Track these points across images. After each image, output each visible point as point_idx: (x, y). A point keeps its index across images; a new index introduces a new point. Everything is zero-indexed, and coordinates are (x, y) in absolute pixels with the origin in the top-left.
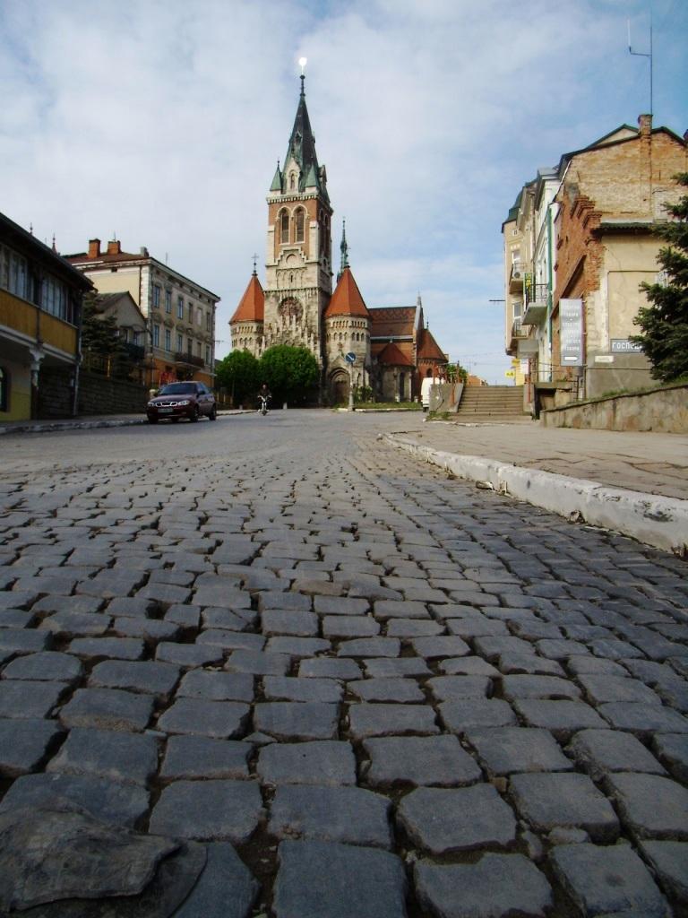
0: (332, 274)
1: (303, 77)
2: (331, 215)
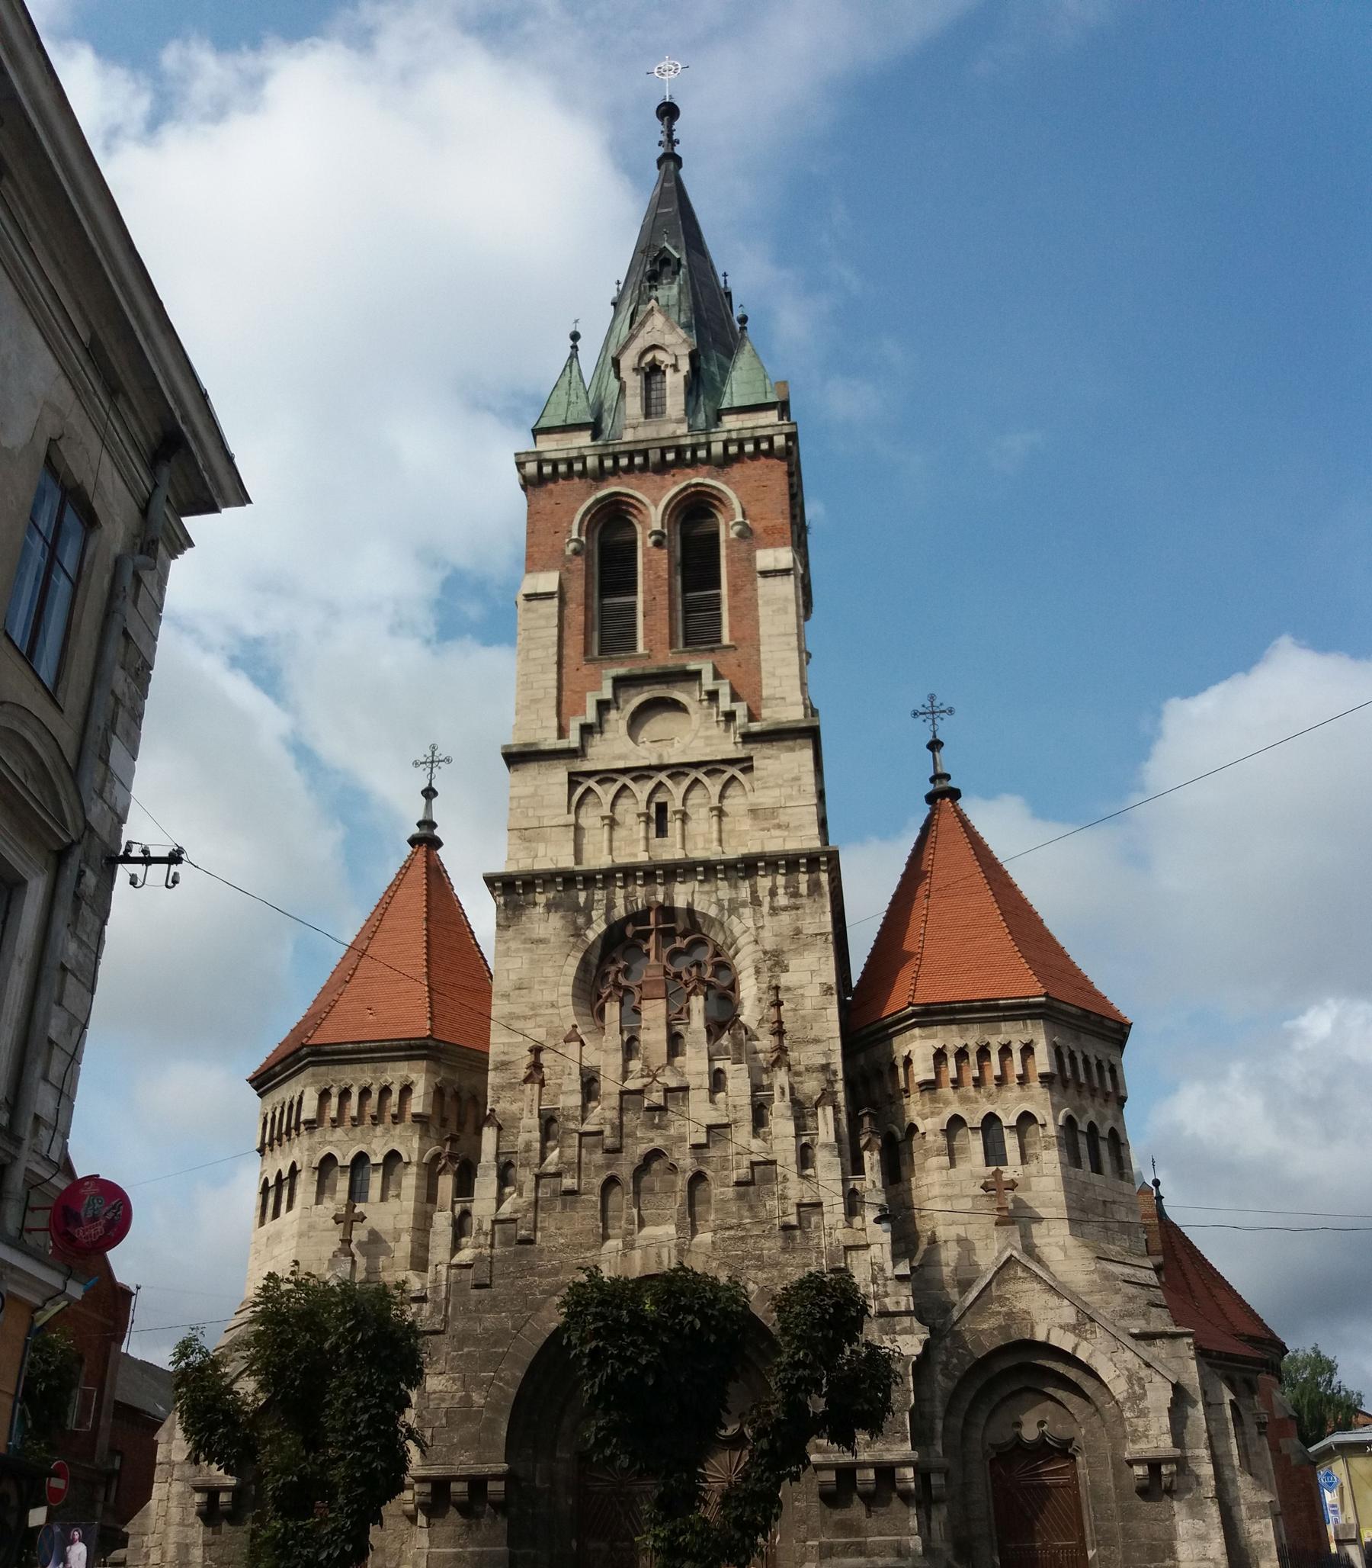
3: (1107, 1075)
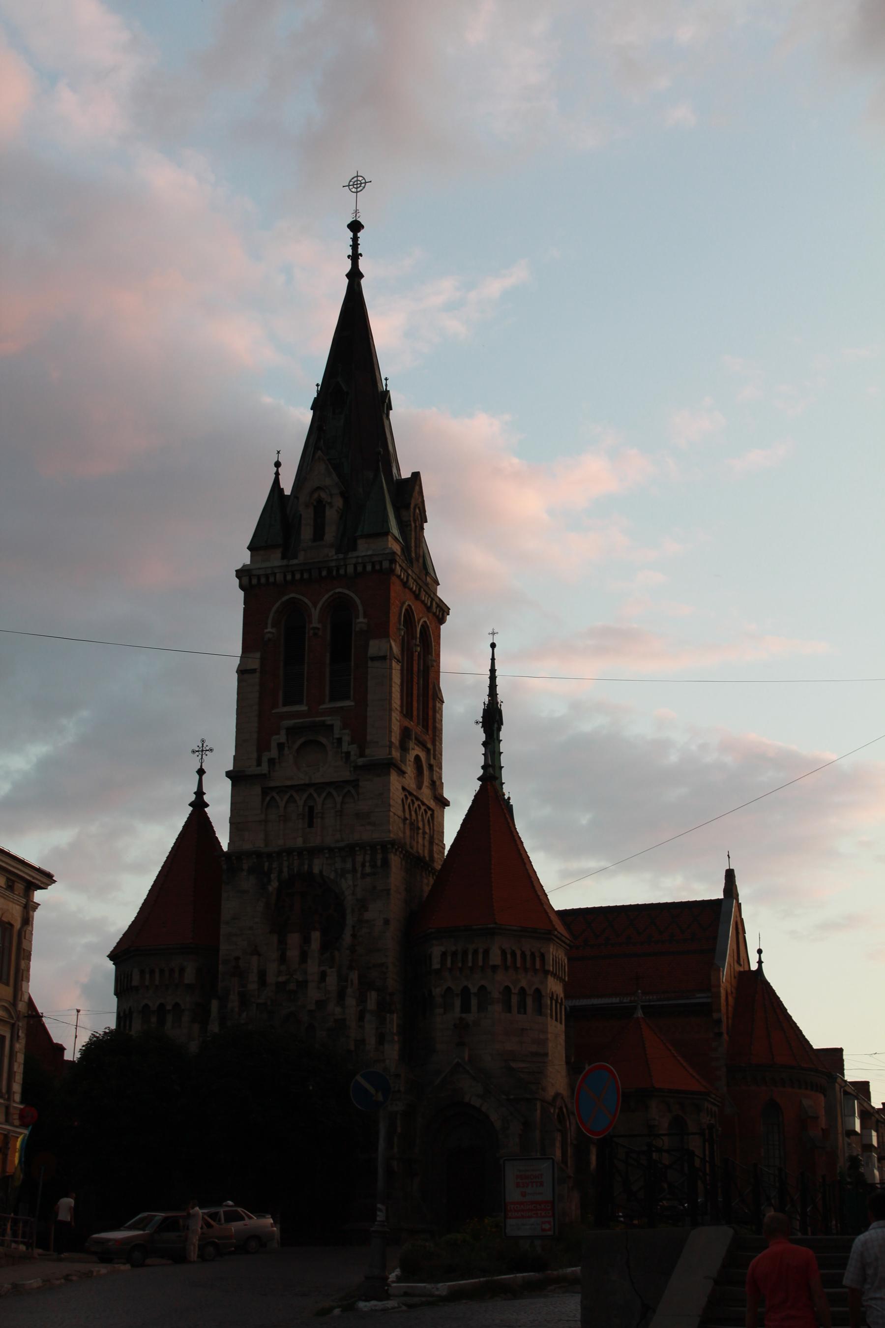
0: (445, 803)
2: (442, 621)
3: (538, 960)
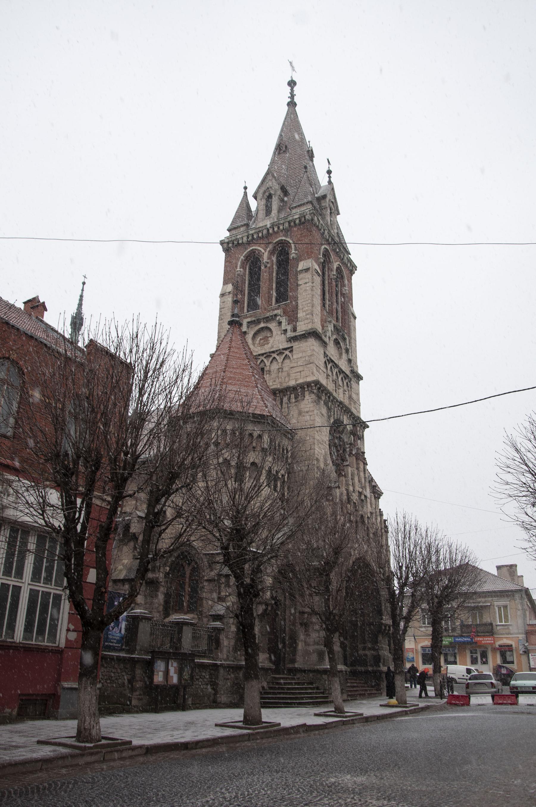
1: (292, 84)
2: (352, 272)
